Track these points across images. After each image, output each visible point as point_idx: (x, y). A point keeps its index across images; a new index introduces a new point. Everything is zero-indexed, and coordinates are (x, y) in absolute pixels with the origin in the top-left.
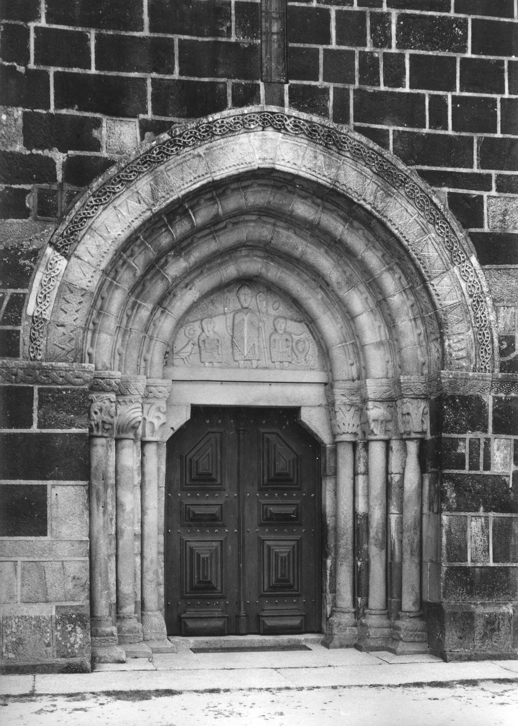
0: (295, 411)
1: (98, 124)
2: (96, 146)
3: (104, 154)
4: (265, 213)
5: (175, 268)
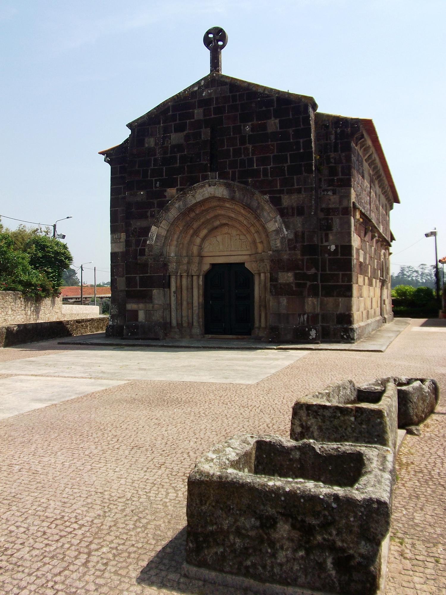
0: (243, 264)
1: (166, 191)
2: (165, 197)
3: (167, 199)
5: (195, 225)
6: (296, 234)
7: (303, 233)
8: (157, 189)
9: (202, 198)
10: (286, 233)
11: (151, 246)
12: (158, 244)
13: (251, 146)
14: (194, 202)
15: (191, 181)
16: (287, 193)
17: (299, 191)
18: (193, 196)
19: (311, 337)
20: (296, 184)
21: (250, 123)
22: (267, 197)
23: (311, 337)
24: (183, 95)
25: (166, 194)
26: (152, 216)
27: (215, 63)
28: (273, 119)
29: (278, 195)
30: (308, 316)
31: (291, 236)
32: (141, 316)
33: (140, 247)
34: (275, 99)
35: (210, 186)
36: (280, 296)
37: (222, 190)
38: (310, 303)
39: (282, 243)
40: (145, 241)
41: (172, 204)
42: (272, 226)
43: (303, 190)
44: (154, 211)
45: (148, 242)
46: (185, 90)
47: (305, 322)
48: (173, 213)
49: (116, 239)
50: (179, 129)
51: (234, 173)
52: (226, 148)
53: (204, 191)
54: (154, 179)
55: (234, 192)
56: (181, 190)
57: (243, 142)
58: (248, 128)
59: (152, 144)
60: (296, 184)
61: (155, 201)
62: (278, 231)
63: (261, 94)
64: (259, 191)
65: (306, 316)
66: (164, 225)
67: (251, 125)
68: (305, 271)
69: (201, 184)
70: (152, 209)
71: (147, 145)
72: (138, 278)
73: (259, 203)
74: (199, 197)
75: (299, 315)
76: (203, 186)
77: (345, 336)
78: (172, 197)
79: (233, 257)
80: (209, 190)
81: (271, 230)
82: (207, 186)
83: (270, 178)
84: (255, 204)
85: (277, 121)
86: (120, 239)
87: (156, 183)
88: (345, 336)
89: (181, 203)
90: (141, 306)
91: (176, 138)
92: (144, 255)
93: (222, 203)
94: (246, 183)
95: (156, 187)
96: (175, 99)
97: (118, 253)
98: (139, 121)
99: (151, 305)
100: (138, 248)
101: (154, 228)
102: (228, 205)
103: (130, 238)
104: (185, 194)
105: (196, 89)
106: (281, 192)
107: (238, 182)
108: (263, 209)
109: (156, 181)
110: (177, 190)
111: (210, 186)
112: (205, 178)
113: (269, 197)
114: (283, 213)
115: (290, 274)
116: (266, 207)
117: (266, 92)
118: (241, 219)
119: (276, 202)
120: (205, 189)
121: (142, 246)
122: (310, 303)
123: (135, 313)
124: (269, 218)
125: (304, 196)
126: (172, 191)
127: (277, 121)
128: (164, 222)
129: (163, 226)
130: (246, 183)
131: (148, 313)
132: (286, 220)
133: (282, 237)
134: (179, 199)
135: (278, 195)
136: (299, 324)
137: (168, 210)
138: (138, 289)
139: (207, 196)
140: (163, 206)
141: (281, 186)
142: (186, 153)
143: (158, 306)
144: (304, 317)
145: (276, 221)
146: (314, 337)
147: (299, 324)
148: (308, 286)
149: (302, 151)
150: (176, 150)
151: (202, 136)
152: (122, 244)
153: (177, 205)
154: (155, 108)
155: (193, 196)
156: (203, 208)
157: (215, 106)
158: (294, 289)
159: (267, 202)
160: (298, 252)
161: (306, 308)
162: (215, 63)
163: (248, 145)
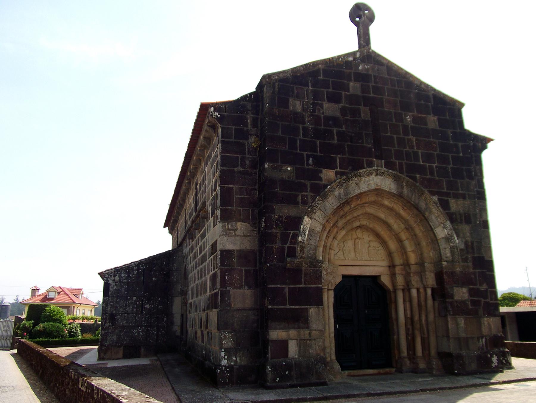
1: (321, 172)
2: (321, 179)
3: (323, 182)
4: (374, 203)
6: (466, 243)
7: (472, 243)
8: (310, 167)
9: (366, 189)
10: (457, 241)
11: (302, 242)
12: (312, 242)
13: (414, 139)
14: (357, 192)
15: (353, 166)
16: (454, 197)
17: (464, 197)
18: (357, 184)
19: (493, 365)
20: (460, 189)
21: (411, 114)
22: (435, 198)
23: (493, 365)
24: (336, 60)
25: (322, 176)
26: (304, 203)
27: (364, 38)
28: (432, 115)
29: (446, 198)
30: (486, 339)
31: (462, 246)
32: (293, 349)
33: (288, 245)
34: (432, 96)
35: (377, 175)
36: (457, 316)
37: (389, 183)
38: (486, 323)
39: (452, 253)
40: (295, 237)
41: (331, 190)
42: (441, 233)
43: (467, 196)
44: (306, 196)
45: (300, 238)
46: (339, 57)
47: (484, 347)
48: (331, 203)
49: (228, 229)
50: (334, 99)
51: (401, 165)
52: (389, 134)
53: (370, 180)
54: (305, 153)
55: (402, 187)
56: (342, 174)
57: (406, 133)
58: (409, 118)
59: (299, 109)
60: (460, 189)
61: (308, 183)
62: (448, 239)
63: (417, 86)
64: (428, 191)
65: (484, 340)
66: (318, 215)
67: (412, 115)
68: (478, 286)
69: (368, 170)
70: (304, 193)
71: (291, 108)
72: (287, 290)
73: (426, 205)
74: (364, 187)
75: (478, 339)
76: (371, 174)
77: (504, 361)
78: (331, 182)
79: (368, 268)
80: (375, 180)
81: (440, 237)
82: (374, 174)
83: (437, 178)
84: (422, 205)
85: (436, 118)
86: (236, 230)
87: (308, 160)
88: (504, 361)
89: (342, 190)
90: (293, 333)
91: (329, 109)
92: (295, 256)
93: (380, 199)
94: (414, 179)
95: (308, 164)
96: (327, 62)
97: (233, 251)
98: (281, 75)
99: (307, 332)
100: (286, 246)
101: (306, 219)
102: (386, 203)
103: (274, 231)
104: (348, 179)
105: (351, 59)
106: (448, 195)
107: (407, 176)
108: (431, 212)
109: (308, 157)
110: (337, 173)
111: (377, 175)
112: (370, 164)
113: (438, 199)
114: (452, 218)
115: (465, 290)
116: (435, 210)
117: (423, 86)
118: (391, 221)
119: (444, 205)
120: (371, 178)
121: (290, 244)
122: (486, 323)
123: (283, 344)
124: (437, 223)
125: (469, 202)
126: (328, 174)
127: (436, 118)
128: (319, 213)
129: (317, 218)
130: (414, 179)
131: (302, 344)
132: (456, 227)
133: (453, 246)
134: (340, 185)
135: (446, 198)
136: (479, 349)
137: (325, 197)
138: (288, 306)
139: (373, 187)
140: (320, 190)
141: (447, 189)
142: (344, 129)
143: (317, 333)
144: (482, 341)
145: (445, 227)
146: (496, 364)
147: (479, 349)
148: (482, 304)
149: (461, 155)
150: (331, 122)
151: (362, 115)
152: (238, 238)
153: (336, 193)
154: (302, 66)
155: (357, 184)
156: (359, 202)
157: (373, 84)
158: (470, 307)
159: (436, 204)
160: (470, 264)
161: (483, 330)
162: (364, 38)
163: (411, 137)
